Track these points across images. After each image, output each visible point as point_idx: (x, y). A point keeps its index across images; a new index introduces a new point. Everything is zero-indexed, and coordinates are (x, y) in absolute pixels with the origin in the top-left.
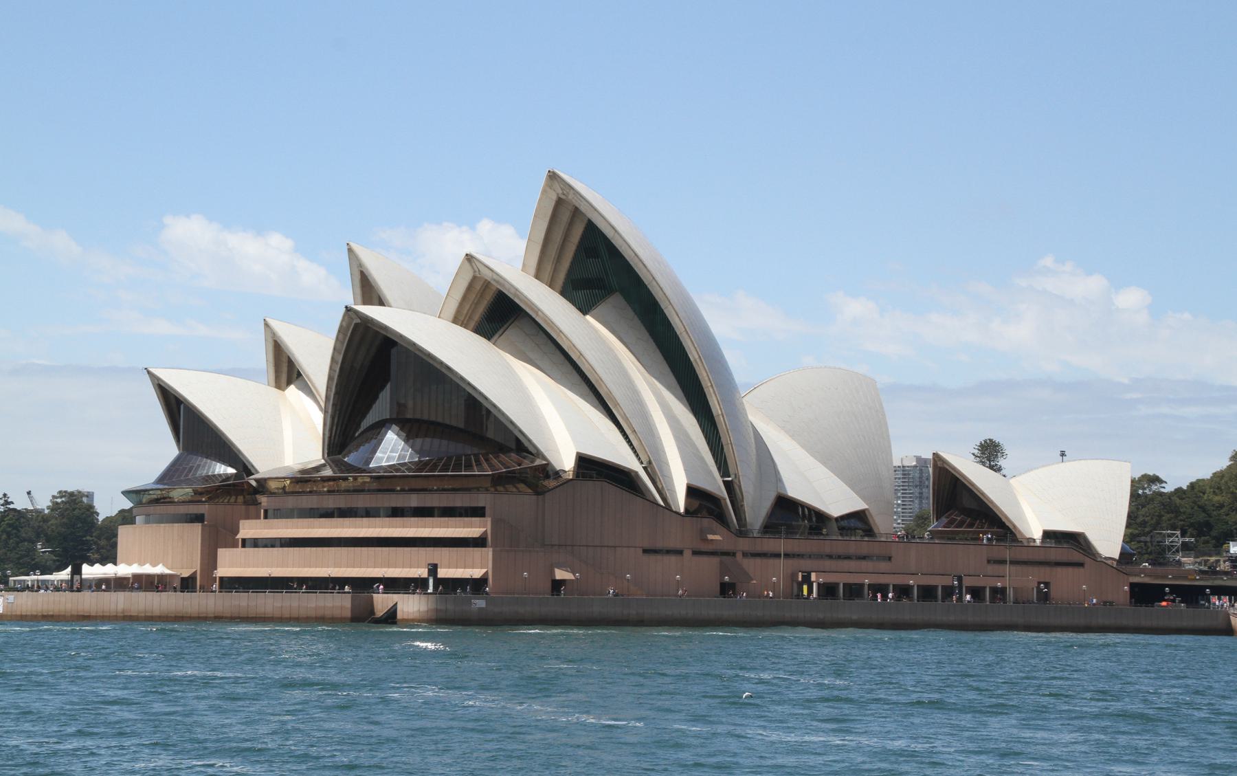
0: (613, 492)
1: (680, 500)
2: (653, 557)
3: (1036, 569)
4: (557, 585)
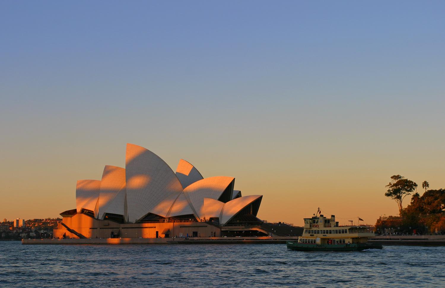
1: (101, 217)
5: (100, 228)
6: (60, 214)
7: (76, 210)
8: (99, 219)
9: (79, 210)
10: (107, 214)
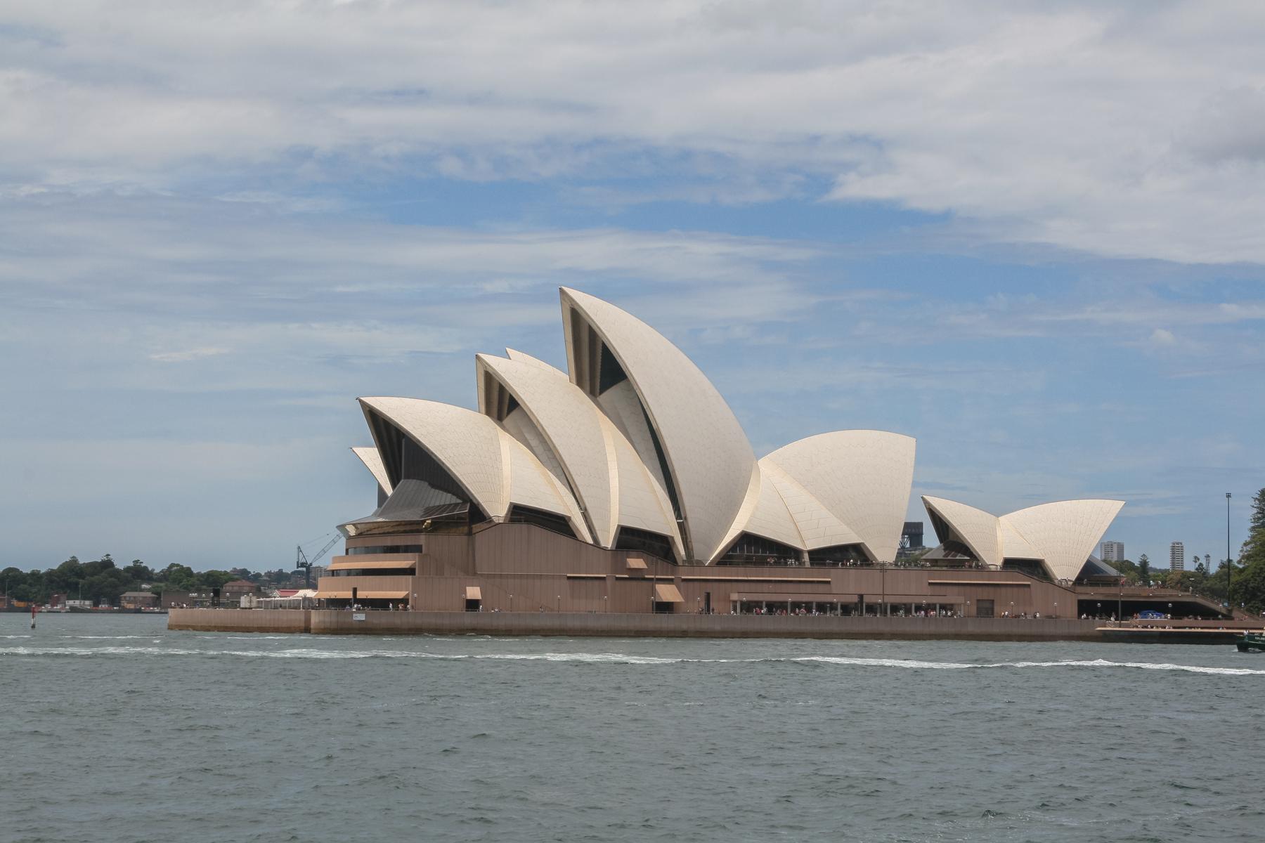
0: (539, 534)
1: (608, 540)
2: (577, 582)
3: (980, 589)
4: (472, 605)
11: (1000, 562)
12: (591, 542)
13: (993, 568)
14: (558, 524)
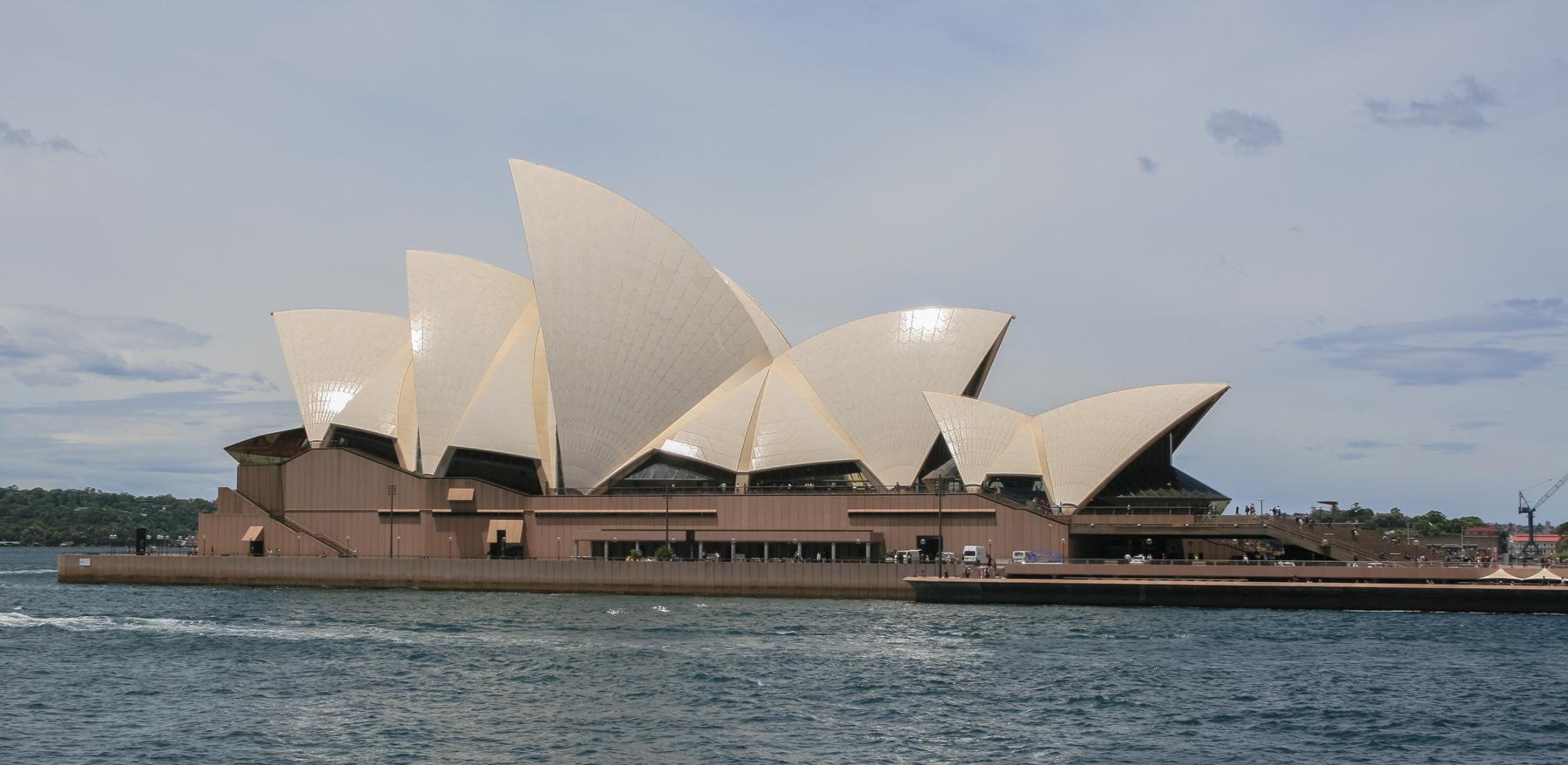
4: (258, 547)
5: (435, 514)
6: (230, 449)
7: (301, 433)
8: (425, 472)
9: (316, 435)
10: (460, 452)
11: (980, 480)
12: (412, 467)
13: (974, 490)
14: (380, 448)
